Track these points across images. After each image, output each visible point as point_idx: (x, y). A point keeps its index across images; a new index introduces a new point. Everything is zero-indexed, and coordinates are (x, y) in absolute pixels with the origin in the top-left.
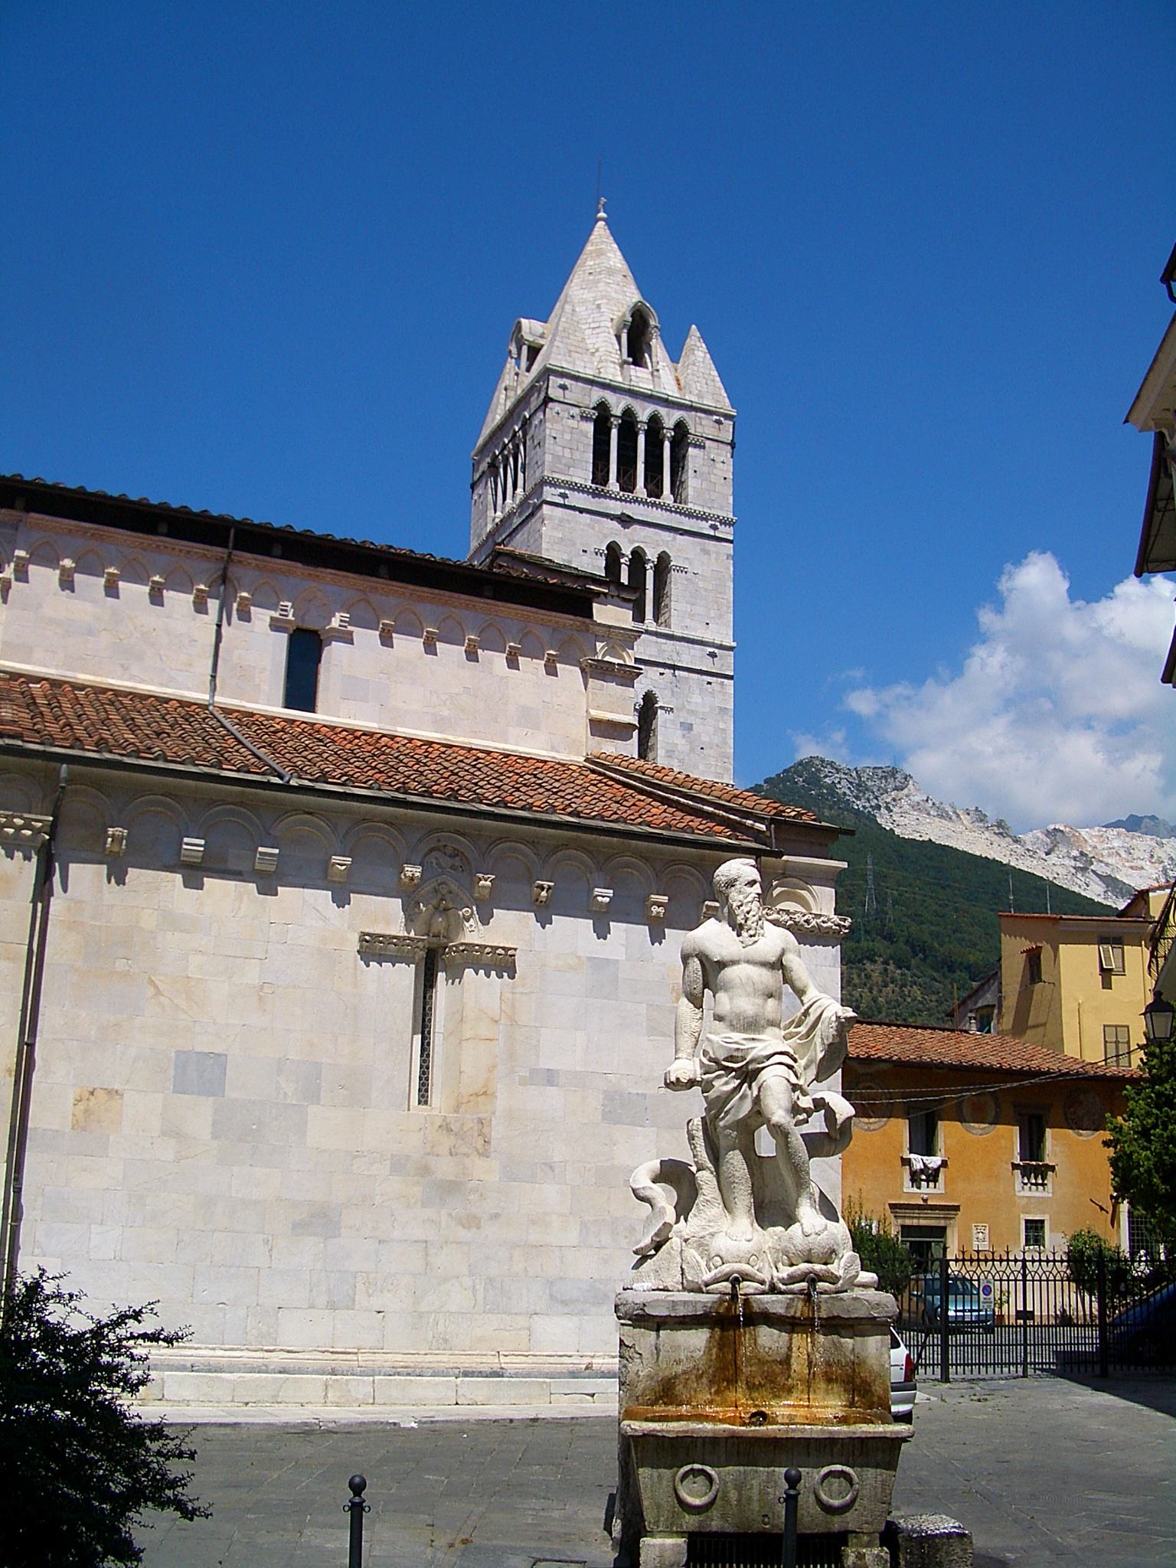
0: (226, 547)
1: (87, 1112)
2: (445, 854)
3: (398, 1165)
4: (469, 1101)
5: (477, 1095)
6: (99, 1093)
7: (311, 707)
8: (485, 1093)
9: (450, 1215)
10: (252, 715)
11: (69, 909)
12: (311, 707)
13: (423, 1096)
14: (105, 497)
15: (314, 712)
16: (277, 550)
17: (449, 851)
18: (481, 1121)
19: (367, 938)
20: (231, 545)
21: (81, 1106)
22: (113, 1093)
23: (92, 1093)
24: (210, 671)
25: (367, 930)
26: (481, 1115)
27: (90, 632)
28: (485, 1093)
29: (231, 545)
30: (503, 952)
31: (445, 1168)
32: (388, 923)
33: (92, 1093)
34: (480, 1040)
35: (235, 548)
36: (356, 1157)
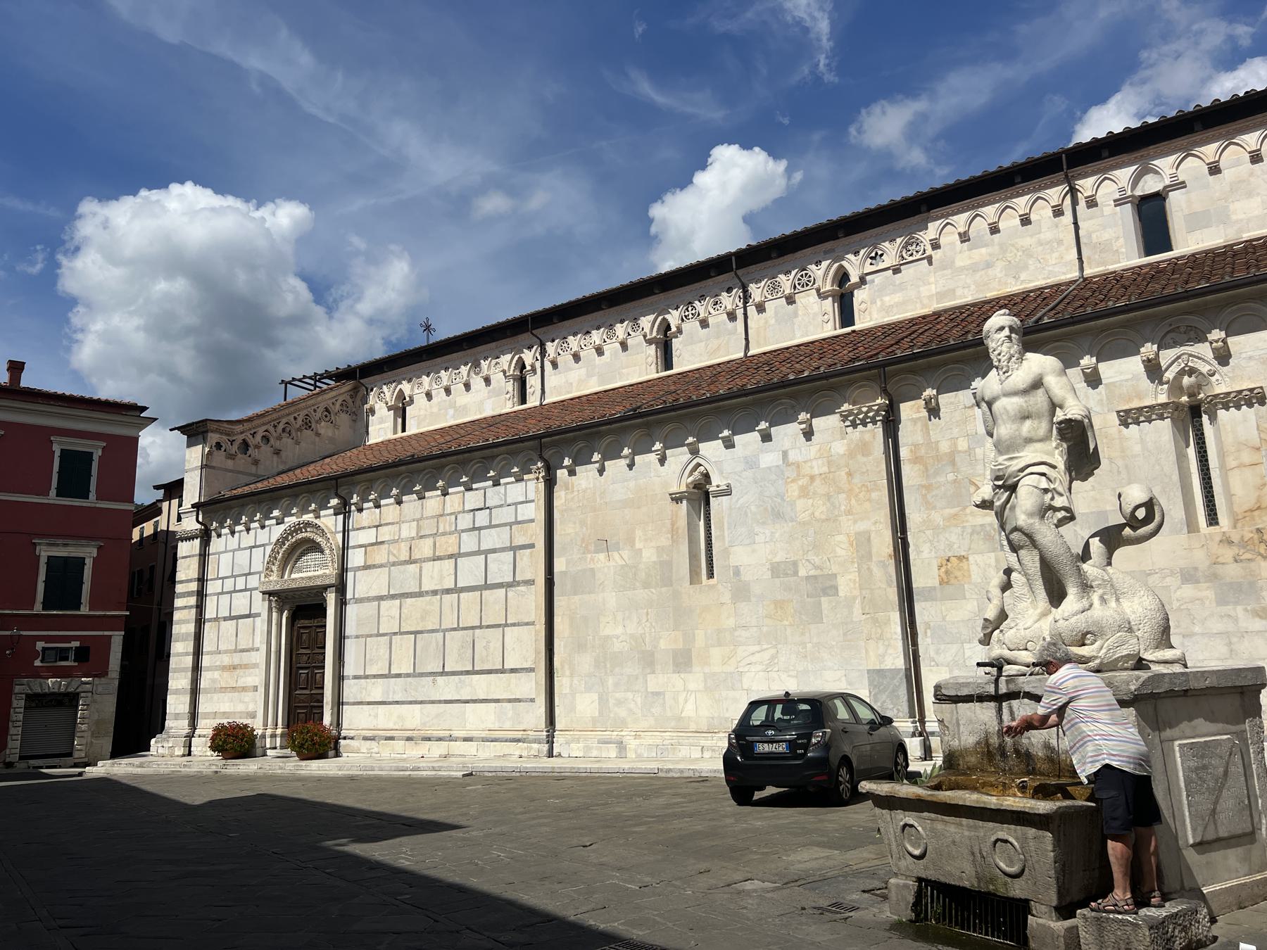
0: (1063, 171)
1: (947, 572)
2: (1181, 333)
3: (1189, 576)
4: (1245, 517)
5: (1252, 511)
6: (953, 559)
7: (1170, 248)
8: (1259, 508)
9: (1246, 610)
10: (1115, 272)
11: (911, 451)
12: (1169, 248)
13: (1213, 519)
14: (975, 178)
15: (1172, 250)
16: (1106, 153)
17: (1182, 330)
18: (1259, 530)
19: (1122, 414)
20: (1065, 167)
21: (943, 569)
22: (961, 558)
23: (948, 560)
24: (1076, 256)
25: (1120, 409)
26: (1259, 526)
27: (989, 265)
28: (1259, 508)
29: (1065, 167)
30: (1248, 393)
31: (1232, 571)
32: (1140, 398)
33: (948, 560)
34: (1245, 466)
35: (1068, 169)
36: (1149, 574)
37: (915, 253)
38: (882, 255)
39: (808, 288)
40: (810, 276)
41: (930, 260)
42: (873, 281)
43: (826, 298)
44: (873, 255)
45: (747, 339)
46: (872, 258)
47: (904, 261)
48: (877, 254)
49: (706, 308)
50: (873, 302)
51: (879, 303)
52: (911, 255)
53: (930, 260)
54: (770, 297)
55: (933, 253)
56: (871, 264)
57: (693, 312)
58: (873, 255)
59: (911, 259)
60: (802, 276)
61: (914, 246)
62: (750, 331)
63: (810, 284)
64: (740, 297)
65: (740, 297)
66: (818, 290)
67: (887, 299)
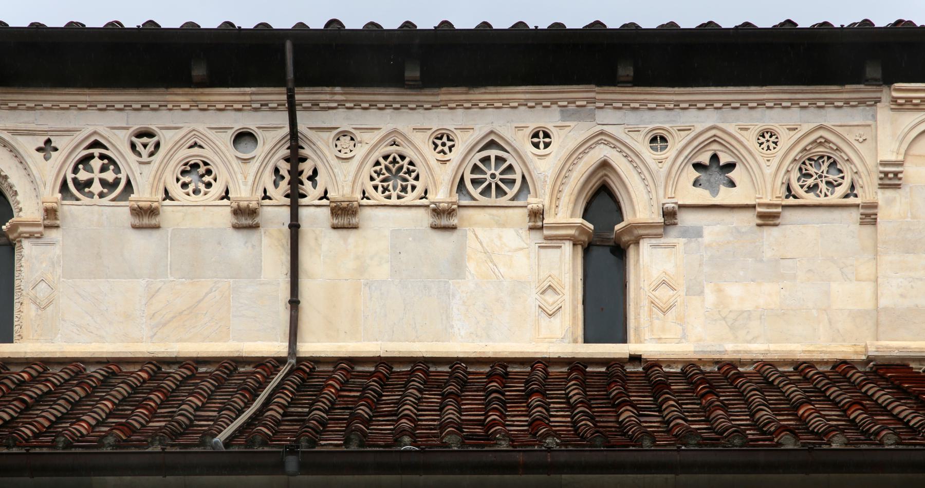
37: (823, 186)
38: (731, 166)
39: (503, 201)
40: (510, 168)
41: (869, 216)
42: (697, 233)
43: (554, 241)
44: (705, 158)
45: (294, 303)
46: (698, 166)
47: (791, 201)
48: (715, 158)
49: (159, 175)
50: (695, 290)
51: (710, 297)
52: (813, 188)
53: (869, 216)
54: (379, 197)
55: (882, 197)
56: (696, 183)
57: (110, 176)
58: (705, 158)
59: (811, 198)
60: (485, 160)
61: (824, 167)
62: (305, 284)
63: (512, 192)
64: (277, 171)
65: (277, 171)
66: (537, 214)
67: (734, 291)
